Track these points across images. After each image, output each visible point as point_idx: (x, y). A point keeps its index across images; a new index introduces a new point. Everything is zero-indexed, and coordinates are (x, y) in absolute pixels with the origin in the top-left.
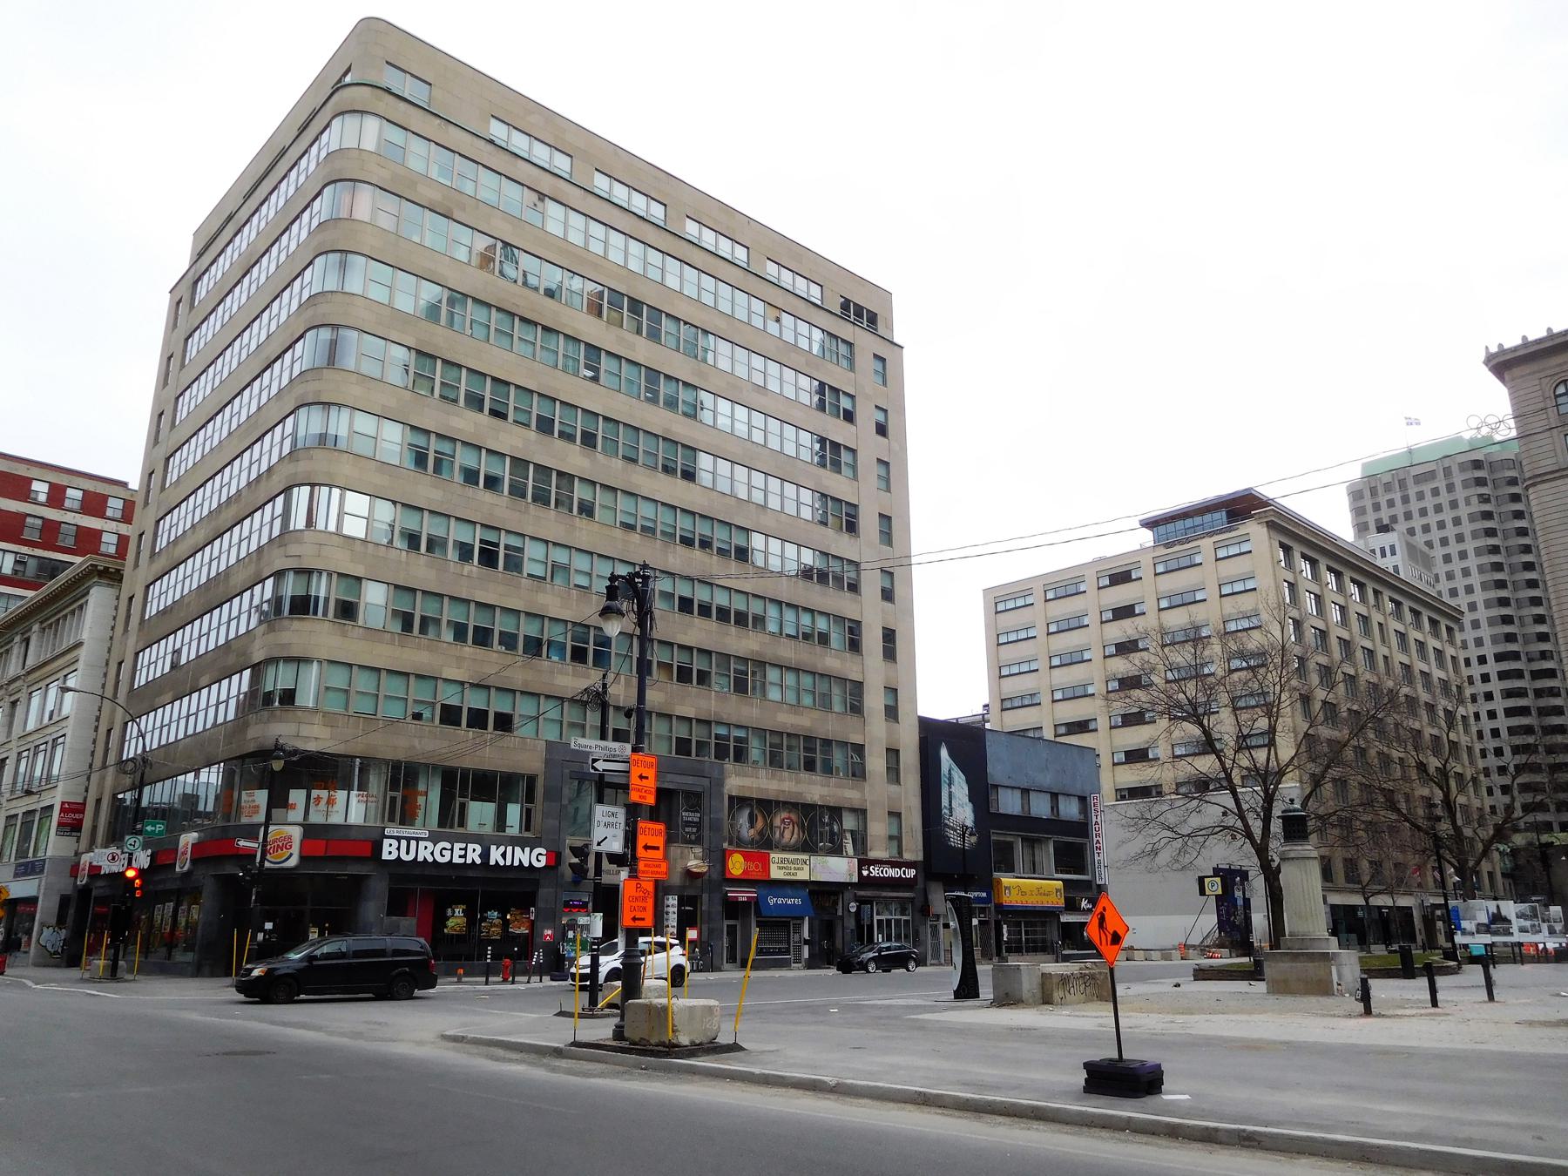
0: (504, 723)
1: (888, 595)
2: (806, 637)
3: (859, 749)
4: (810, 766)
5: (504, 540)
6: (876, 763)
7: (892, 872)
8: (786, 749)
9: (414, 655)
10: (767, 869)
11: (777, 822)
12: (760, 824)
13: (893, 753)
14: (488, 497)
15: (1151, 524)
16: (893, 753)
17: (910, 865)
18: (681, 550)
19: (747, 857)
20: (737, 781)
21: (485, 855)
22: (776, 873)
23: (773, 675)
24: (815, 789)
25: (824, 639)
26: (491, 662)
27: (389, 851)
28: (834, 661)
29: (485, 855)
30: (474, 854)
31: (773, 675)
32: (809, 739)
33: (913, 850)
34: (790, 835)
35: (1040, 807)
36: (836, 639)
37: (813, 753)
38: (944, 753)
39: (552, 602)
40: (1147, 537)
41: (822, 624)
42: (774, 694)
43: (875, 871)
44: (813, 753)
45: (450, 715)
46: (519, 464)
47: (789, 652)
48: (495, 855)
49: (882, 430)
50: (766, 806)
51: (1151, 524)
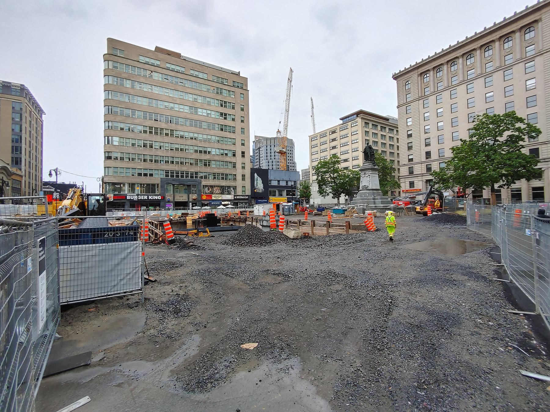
0: (151, 175)
1: (243, 144)
2: (223, 154)
3: (235, 175)
4: (223, 178)
5: (148, 142)
6: (239, 177)
7: (242, 197)
8: (215, 176)
9: (131, 165)
10: (211, 198)
11: (215, 189)
12: (210, 190)
13: (243, 176)
14: (144, 135)
15: (342, 119)
16: (243, 176)
17: (246, 196)
18: (191, 141)
19: (207, 196)
20: (204, 182)
21: (148, 197)
22: (213, 198)
23: (213, 162)
24: (224, 183)
25: (226, 154)
26: (148, 165)
27: (128, 198)
28: (230, 158)
29: (148, 197)
30: (146, 197)
31: (213, 162)
32: (223, 174)
33: (248, 192)
34: (218, 191)
35: (283, 184)
36: (230, 154)
37: (225, 177)
38: (256, 175)
39: (160, 153)
40: (341, 122)
41: (226, 152)
42: (214, 166)
43: (238, 197)
44: (225, 177)
45: (140, 174)
46: (151, 128)
47: (217, 158)
48: (150, 198)
49: (242, 110)
50: (212, 187)
51: (342, 119)
